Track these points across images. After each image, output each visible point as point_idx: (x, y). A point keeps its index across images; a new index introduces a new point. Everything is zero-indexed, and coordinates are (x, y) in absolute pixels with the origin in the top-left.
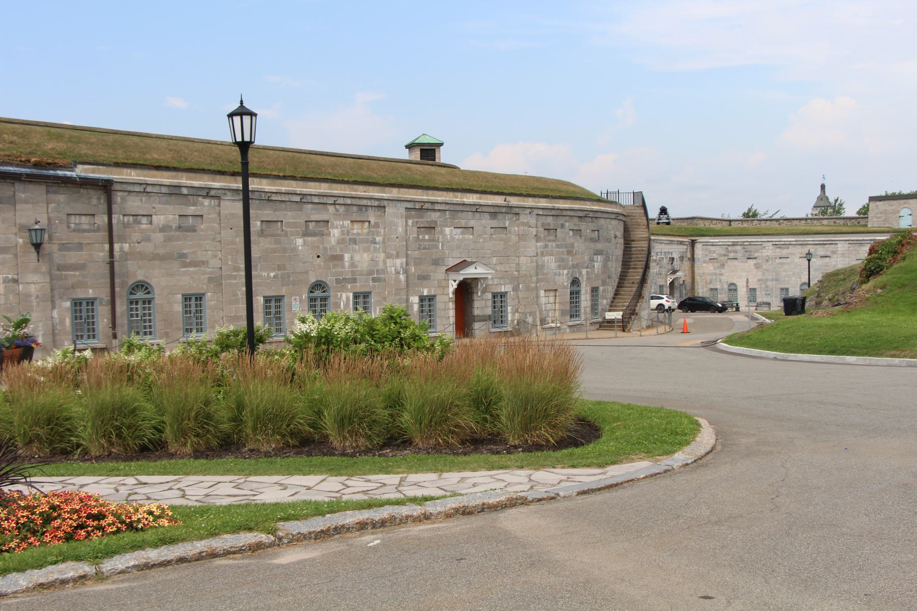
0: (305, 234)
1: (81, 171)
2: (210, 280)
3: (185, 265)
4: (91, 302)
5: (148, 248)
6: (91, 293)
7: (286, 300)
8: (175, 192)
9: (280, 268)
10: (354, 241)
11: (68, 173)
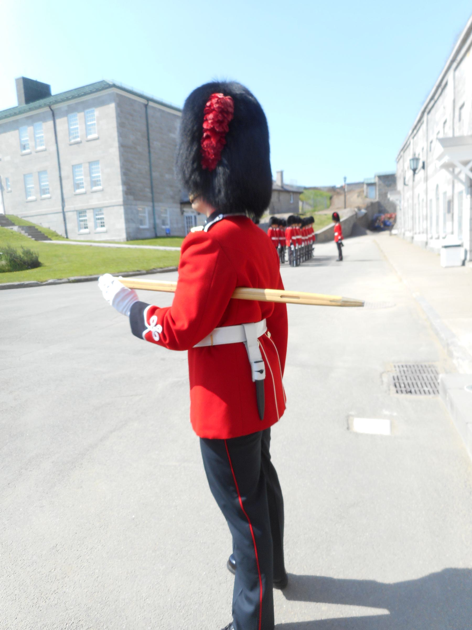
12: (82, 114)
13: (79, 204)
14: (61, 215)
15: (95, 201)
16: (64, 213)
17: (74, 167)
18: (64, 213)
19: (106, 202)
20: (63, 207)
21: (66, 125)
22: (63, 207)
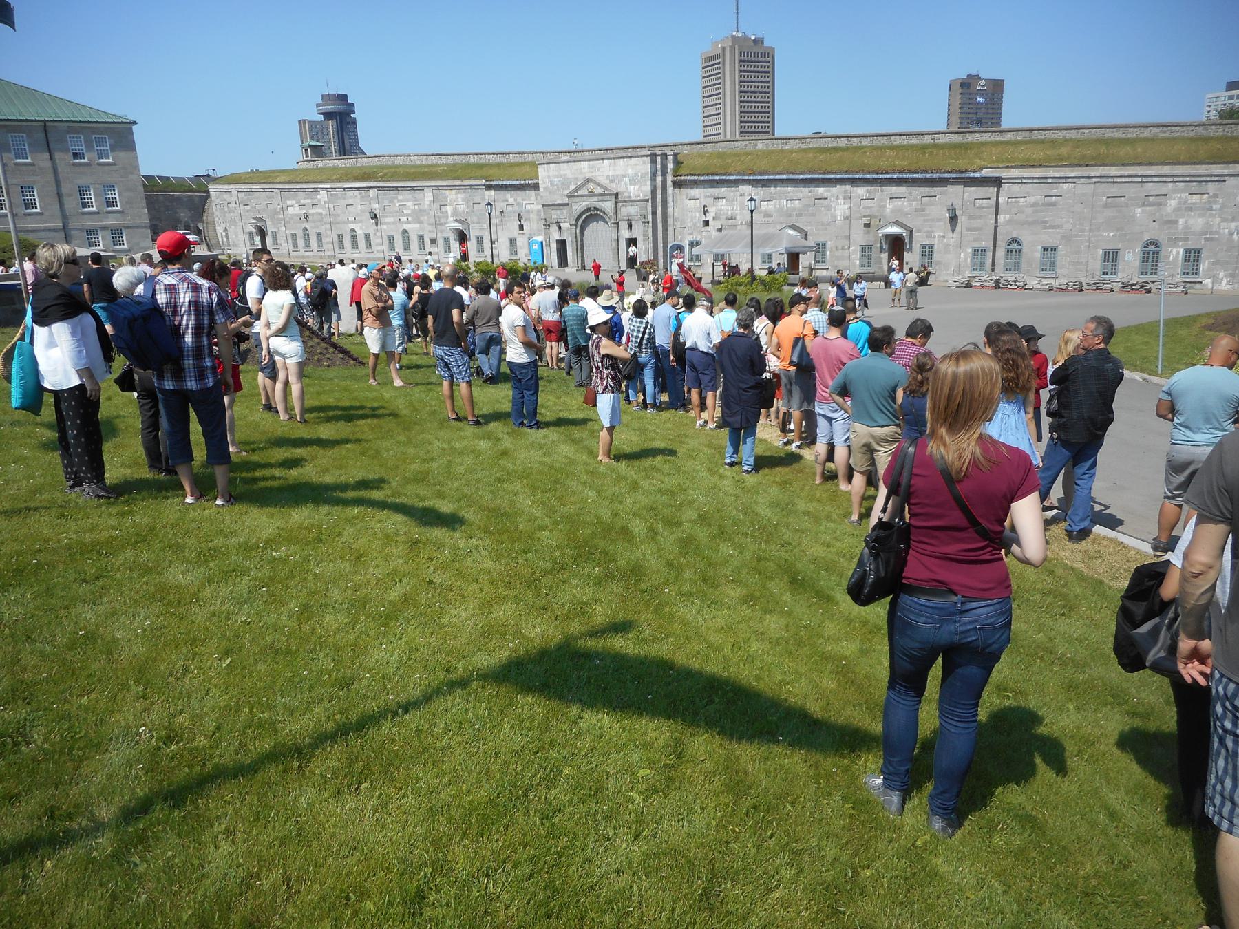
0: (1143, 205)
1: (985, 173)
2: (1063, 237)
3: (1046, 228)
4: (984, 250)
5: (1022, 217)
6: (984, 244)
7: (1121, 253)
8: (1043, 180)
9: (1118, 230)
10: (1191, 209)
11: (977, 175)
13: (89, 223)
15: (111, 221)
19: (128, 222)
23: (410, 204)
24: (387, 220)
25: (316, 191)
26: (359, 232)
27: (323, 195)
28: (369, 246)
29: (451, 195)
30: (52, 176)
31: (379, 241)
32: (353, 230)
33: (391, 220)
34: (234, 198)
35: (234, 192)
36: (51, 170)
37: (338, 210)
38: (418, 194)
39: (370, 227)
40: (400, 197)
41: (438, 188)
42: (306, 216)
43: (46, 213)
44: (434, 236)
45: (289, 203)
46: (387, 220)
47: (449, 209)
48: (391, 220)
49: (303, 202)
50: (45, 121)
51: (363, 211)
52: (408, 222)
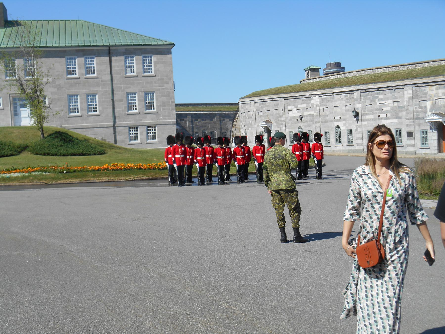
12: (140, 57)
13: (132, 122)
14: (112, 130)
15: (149, 121)
16: (114, 127)
17: (128, 94)
18: (114, 127)
19: (160, 121)
20: (115, 122)
21: (123, 63)
22: (115, 122)
23: (390, 102)
24: (368, 117)
25: (310, 97)
26: (343, 129)
27: (316, 100)
28: (350, 140)
29: (432, 91)
30: (110, 86)
31: (360, 135)
32: (338, 127)
33: (371, 117)
34: (253, 108)
35: (253, 103)
36: (110, 82)
37: (327, 112)
38: (398, 93)
39: (352, 123)
40: (381, 97)
41: (418, 85)
42: (301, 117)
43: (103, 115)
44: (411, 129)
45: (290, 108)
46: (368, 117)
47: (428, 104)
48: (371, 117)
49: (300, 106)
50: (109, 46)
51: (347, 111)
52: (387, 118)
